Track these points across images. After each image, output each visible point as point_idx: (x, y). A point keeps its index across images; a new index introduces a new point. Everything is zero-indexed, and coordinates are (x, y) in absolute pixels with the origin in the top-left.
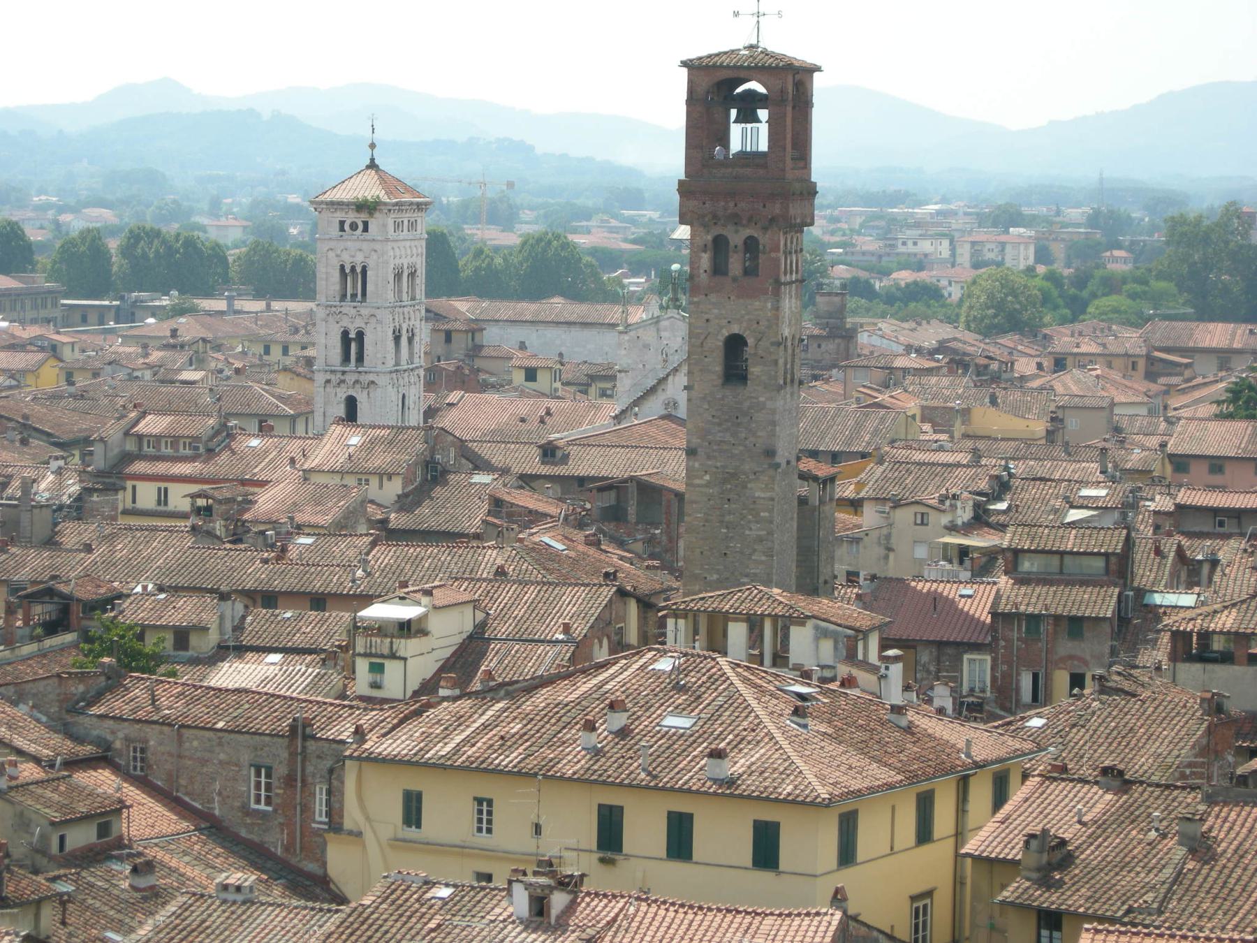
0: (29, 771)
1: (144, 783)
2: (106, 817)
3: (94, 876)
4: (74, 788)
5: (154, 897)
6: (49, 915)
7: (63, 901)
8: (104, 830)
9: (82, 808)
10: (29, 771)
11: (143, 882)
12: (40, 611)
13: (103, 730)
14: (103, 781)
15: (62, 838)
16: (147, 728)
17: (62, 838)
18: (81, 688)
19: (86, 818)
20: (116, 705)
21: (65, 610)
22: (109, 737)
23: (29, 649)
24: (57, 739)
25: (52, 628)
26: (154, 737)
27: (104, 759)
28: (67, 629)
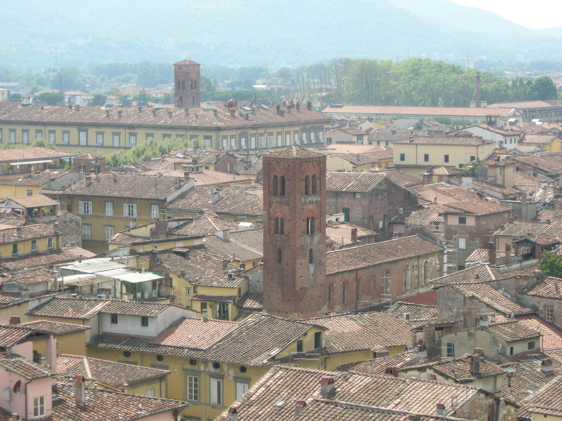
0: (500, 319)
1: (552, 325)
2: (532, 340)
3: (525, 366)
4: (520, 327)
5: (551, 374)
6: (501, 382)
7: (510, 376)
8: (531, 345)
9: (521, 336)
10: (500, 319)
11: (547, 369)
12: (524, 250)
13: (534, 301)
14: (533, 324)
15: (512, 349)
16: (554, 301)
17: (512, 349)
18: (526, 283)
19: (523, 340)
20: (541, 290)
21: (533, 249)
22: (537, 305)
23: (518, 265)
24: (513, 305)
25: (527, 257)
26: (556, 305)
27: (534, 314)
28: (534, 257)
